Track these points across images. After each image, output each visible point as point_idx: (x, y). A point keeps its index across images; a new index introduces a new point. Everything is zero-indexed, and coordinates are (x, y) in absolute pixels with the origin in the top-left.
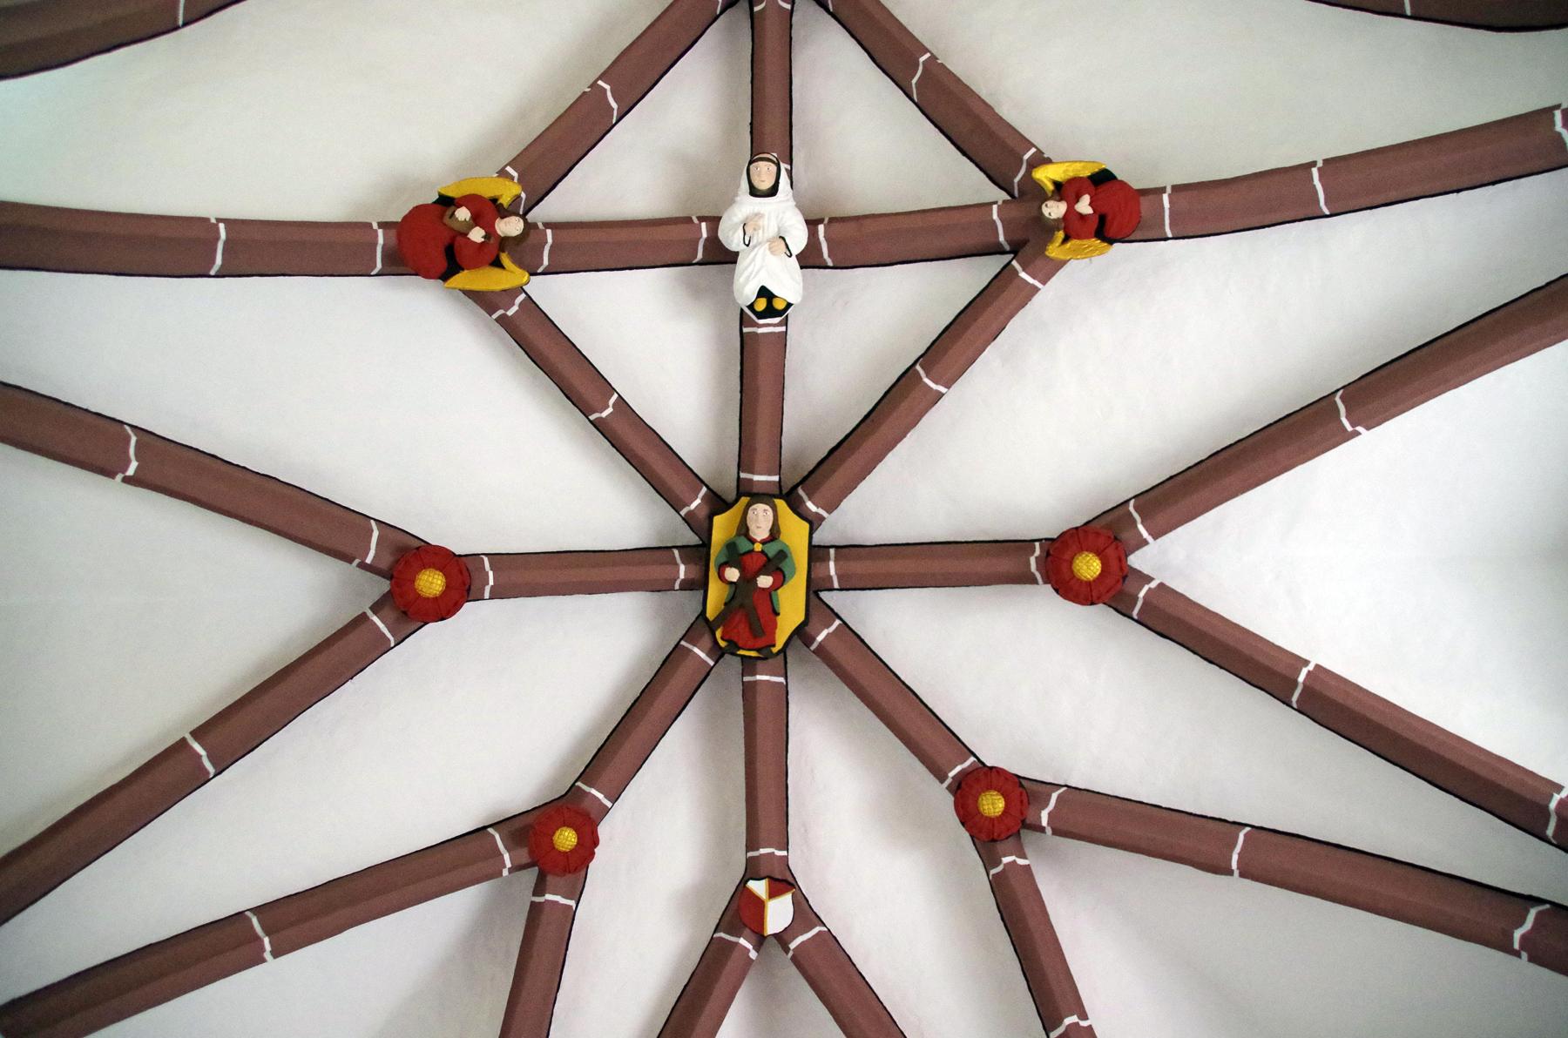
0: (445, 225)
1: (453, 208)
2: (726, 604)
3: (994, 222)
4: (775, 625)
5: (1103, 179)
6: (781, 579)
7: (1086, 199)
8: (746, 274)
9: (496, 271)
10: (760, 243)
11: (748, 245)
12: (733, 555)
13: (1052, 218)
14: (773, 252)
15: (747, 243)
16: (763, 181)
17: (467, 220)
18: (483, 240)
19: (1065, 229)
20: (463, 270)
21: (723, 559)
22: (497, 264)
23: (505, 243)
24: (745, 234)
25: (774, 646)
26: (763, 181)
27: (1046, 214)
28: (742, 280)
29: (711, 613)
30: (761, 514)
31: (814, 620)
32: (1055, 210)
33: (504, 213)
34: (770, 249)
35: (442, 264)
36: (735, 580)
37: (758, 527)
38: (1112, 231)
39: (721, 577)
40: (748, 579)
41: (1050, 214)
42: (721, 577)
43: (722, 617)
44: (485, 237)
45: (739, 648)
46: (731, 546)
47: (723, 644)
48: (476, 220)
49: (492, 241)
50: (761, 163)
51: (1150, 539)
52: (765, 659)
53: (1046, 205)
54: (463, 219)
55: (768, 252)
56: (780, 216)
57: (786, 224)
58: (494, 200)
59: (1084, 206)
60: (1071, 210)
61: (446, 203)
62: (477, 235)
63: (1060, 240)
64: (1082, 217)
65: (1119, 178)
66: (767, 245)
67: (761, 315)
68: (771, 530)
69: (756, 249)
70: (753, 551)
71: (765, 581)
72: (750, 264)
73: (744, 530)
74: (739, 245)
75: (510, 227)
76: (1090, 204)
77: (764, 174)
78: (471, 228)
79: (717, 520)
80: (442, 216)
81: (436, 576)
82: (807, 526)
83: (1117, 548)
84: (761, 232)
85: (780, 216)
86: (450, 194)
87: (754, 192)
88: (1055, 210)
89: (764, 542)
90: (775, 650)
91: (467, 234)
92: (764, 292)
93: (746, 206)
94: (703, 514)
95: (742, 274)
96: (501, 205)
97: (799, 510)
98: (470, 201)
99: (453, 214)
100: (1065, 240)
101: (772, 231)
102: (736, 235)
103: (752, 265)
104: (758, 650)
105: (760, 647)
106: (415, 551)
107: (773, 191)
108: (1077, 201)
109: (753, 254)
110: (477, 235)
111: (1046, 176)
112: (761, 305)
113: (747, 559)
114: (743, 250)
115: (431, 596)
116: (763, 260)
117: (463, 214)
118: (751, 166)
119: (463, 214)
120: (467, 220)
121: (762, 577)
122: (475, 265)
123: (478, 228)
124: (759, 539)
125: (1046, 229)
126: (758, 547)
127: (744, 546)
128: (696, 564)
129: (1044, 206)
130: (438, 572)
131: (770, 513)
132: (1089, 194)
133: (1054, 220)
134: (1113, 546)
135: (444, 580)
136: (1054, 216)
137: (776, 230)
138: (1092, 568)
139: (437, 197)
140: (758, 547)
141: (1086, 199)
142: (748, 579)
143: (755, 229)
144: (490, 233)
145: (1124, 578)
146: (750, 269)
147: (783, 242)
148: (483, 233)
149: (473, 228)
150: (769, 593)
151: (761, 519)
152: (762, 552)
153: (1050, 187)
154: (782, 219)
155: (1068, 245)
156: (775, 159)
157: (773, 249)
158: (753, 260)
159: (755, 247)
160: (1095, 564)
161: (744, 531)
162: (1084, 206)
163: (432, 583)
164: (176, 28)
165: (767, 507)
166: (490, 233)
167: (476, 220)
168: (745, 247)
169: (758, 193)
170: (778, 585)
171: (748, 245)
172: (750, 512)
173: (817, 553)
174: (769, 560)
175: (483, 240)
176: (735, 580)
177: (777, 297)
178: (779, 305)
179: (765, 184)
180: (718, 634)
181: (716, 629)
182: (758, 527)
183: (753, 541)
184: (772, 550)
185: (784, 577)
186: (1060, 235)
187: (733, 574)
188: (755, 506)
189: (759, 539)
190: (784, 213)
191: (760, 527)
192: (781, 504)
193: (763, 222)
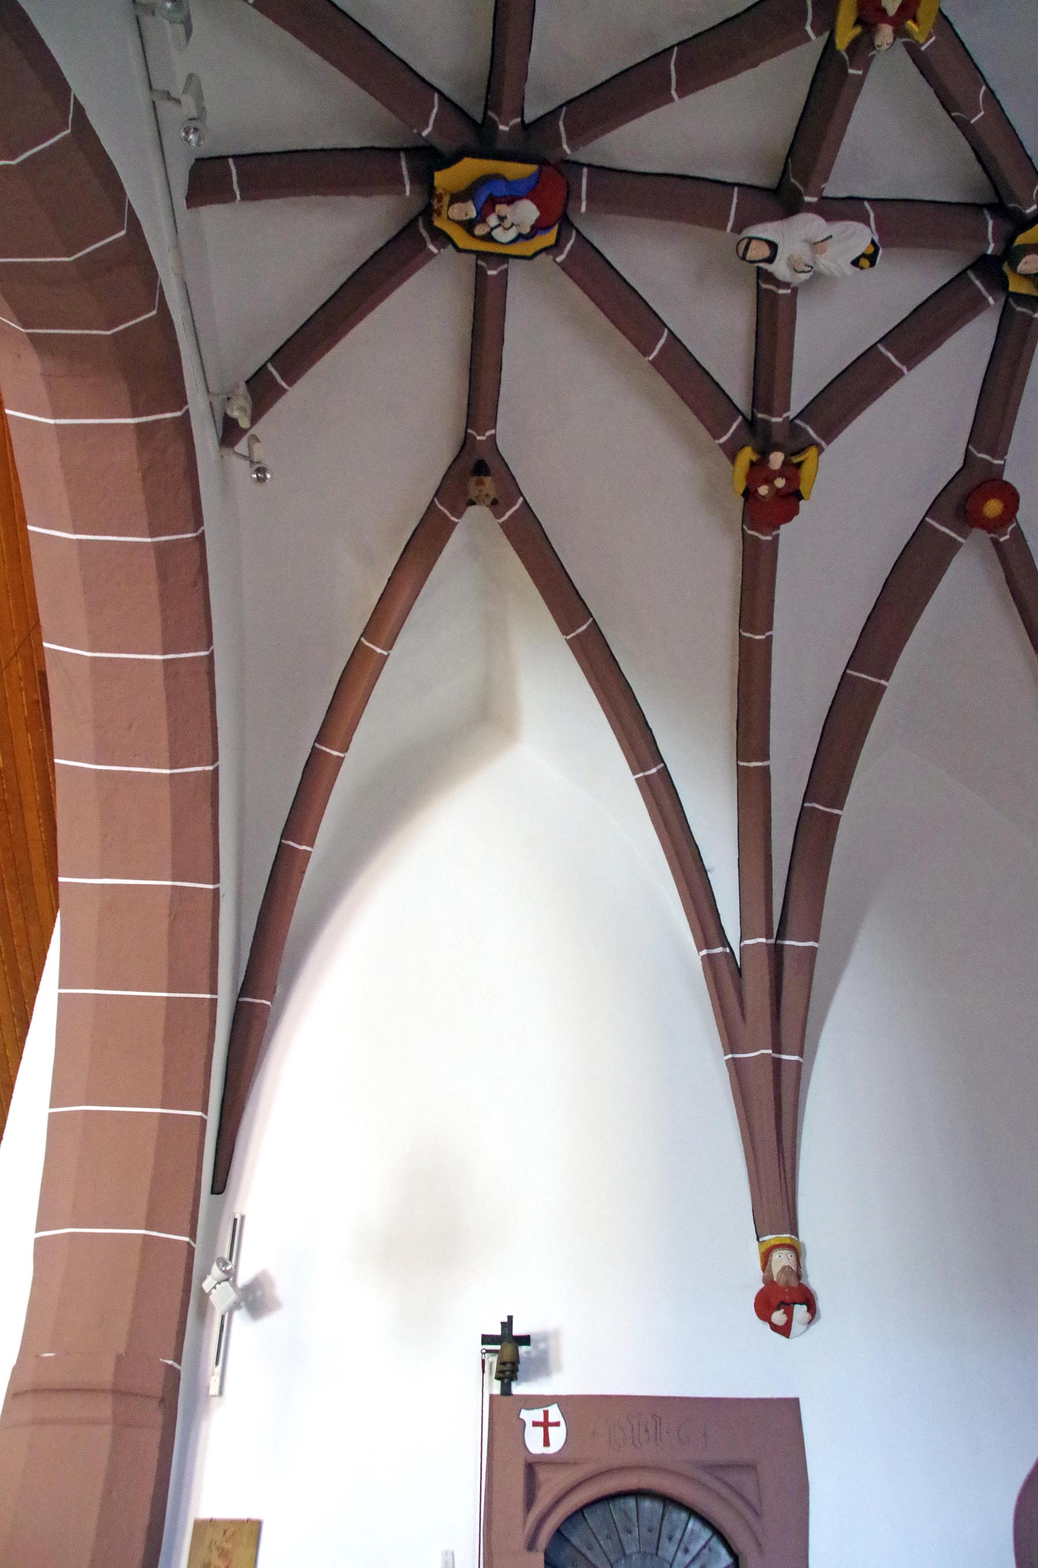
14: (823, 251)
15: (810, 269)
24: (803, 272)
44: (782, 478)
48: (769, 481)
55: (824, 255)
61: (749, 494)
78: (774, 486)
87: (771, 260)
99: (763, 497)
107: (773, 246)
117: (763, 490)
119: (763, 490)
156: (745, 242)
165: (1024, 260)
166: (780, 473)
167: (769, 481)
171: (812, 268)
179: (766, 252)
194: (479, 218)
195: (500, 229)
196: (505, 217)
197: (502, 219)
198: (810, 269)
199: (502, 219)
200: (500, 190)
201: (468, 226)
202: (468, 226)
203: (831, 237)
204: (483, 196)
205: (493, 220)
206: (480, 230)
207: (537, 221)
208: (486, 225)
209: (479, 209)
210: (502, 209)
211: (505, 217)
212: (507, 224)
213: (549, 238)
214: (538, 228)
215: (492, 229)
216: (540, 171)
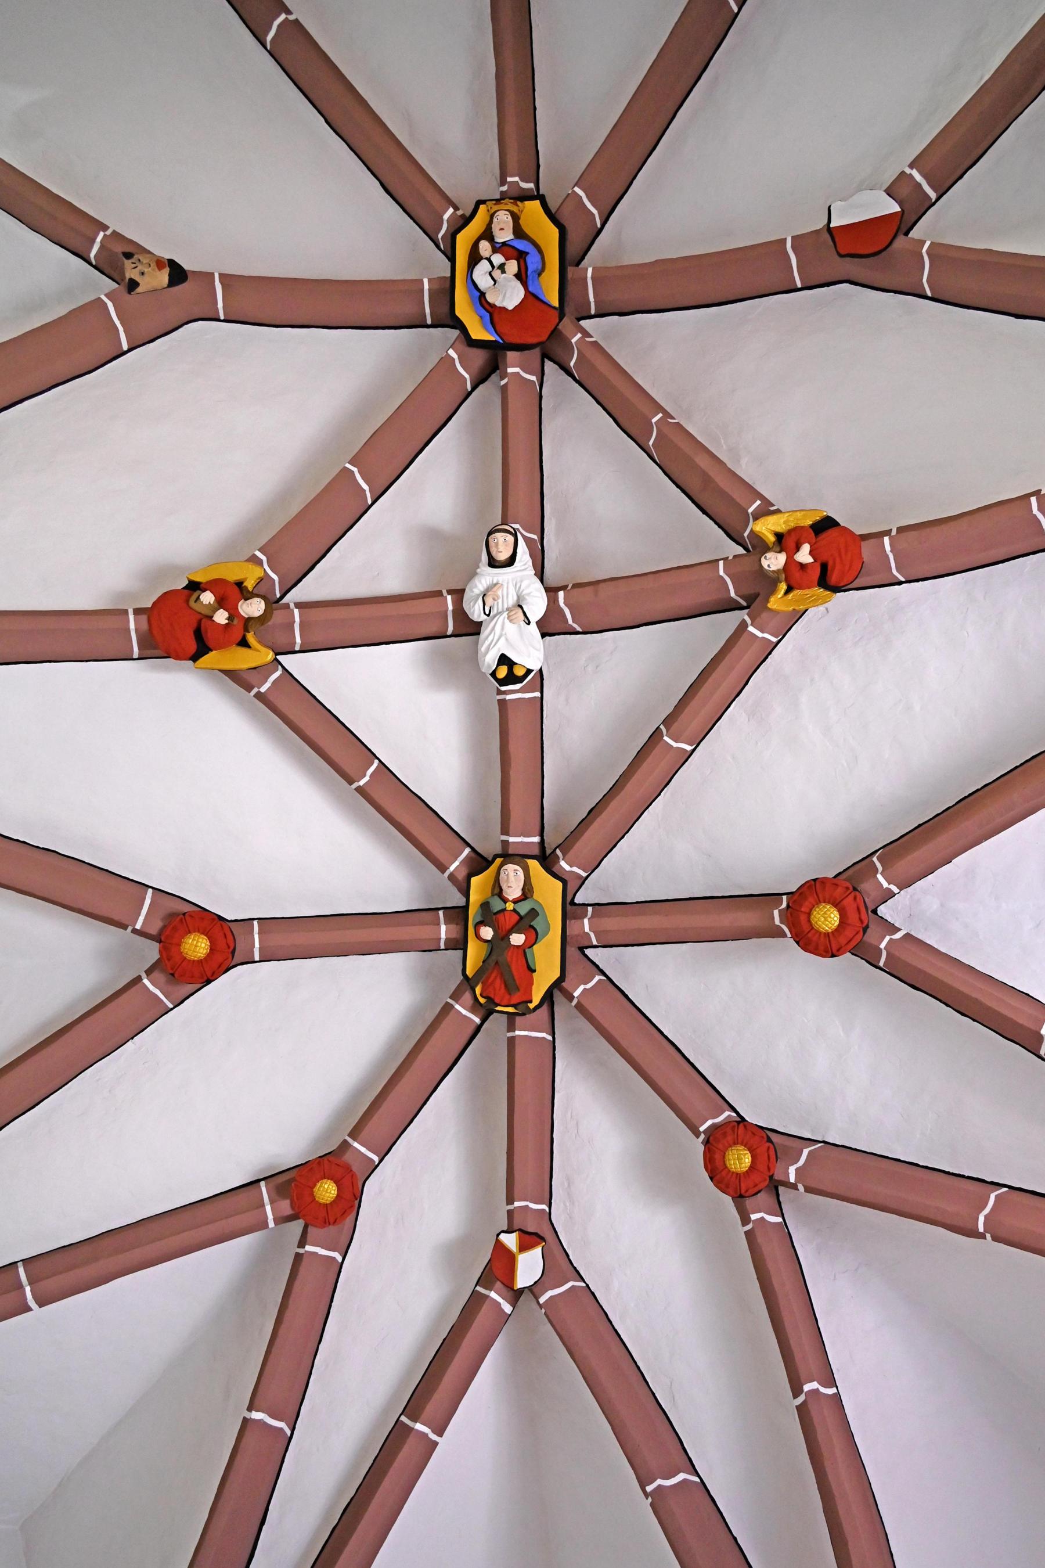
0: (191, 608)
1: (198, 592)
2: (483, 962)
4: (531, 983)
6: (534, 937)
7: (806, 548)
8: (487, 643)
10: (500, 612)
12: (488, 916)
13: (771, 569)
15: (487, 613)
16: (501, 552)
17: (212, 603)
18: (227, 621)
19: (786, 580)
20: (212, 651)
21: (479, 919)
22: (244, 643)
23: (248, 622)
24: (484, 604)
25: (531, 1002)
26: (501, 552)
27: (766, 567)
28: (483, 649)
29: (470, 972)
30: (512, 874)
31: (570, 976)
32: (775, 561)
33: (247, 595)
34: (508, 618)
35: (192, 647)
36: (489, 938)
37: (509, 887)
38: (833, 579)
39: (477, 935)
40: (502, 938)
41: (769, 566)
42: (477, 935)
43: (480, 973)
44: (228, 619)
45: (497, 1005)
46: (485, 906)
47: (482, 1000)
48: (221, 602)
49: (235, 622)
50: (498, 535)
52: (523, 1014)
53: (765, 558)
54: (207, 603)
55: (507, 621)
56: (518, 586)
57: (524, 593)
58: (239, 584)
59: (804, 556)
60: (790, 560)
61: (194, 587)
62: (221, 617)
63: (782, 592)
64: (803, 566)
66: (505, 614)
67: (503, 682)
68: (522, 890)
69: (497, 618)
70: (505, 910)
71: (517, 939)
72: (490, 634)
73: (498, 890)
74: (479, 616)
75: (253, 608)
76: (811, 553)
78: (215, 610)
79: (474, 880)
80: (187, 601)
81: (201, 940)
82: (560, 884)
83: (855, 898)
84: (500, 601)
85: (518, 586)
86: (197, 579)
87: (493, 563)
88: (775, 561)
89: (516, 901)
90: (532, 1006)
91: (212, 617)
92: (504, 660)
93: (487, 576)
94: (461, 876)
96: (246, 588)
97: (554, 870)
98: (214, 585)
99: (198, 598)
100: (787, 592)
101: (512, 600)
102: (476, 607)
103: (493, 634)
104: (514, 1006)
105: (515, 1003)
106: (182, 916)
107: (511, 561)
108: (798, 549)
110: (221, 617)
111: (767, 528)
112: (502, 673)
113: (501, 916)
114: (486, 620)
115: (196, 959)
116: (503, 628)
117: (208, 598)
118: (489, 538)
120: (212, 603)
121: (514, 934)
122: (221, 646)
123: (222, 610)
124: (511, 898)
125: (770, 581)
126: (510, 906)
127: (497, 905)
128: (457, 924)
129: (763, 558)
130: (203, 936)
131: (521, 873)
132: (809, 543)
134: (851, 897)
135: (208, 943)
136: (773, 568)
137: (515, 598)
138: (829, 919)
139: (187, 582)
140: (510, 906)
141: (806, 548)
142: (502, 938)
143: (494, 599)
144: (233, 615)
145: (865, 929)
146: (490, 638)
147: (520, 611)
148: (226, 614)
149: (218, 610)
150: (523, 950)
151: (513, 879)
152: (514, 910)
153: (772, 539)
154: (520, 587)
155: (790, 596)
157: (511, 618)
158: (493, 629)
159: (495, 616)
160: (832, 916)
161: (497, 891)
162: (804, 556)
163: (196, 946)
165: (517, 867)
166: (233, 615)
167: (221, 602)
168: (486, 617)
169: (497, 564)
170: (530, 943)
171: (488, 615)
172: (502, 871)
173: (570, 909)
174: (521, 918)
175: (227, 621)
176: (490, 939)
177: (516, 664)
178: (519, 672)
179: (503, 555)
180: (478, 990)
181: (476, 985)
182: (509, 887)
183: (505, 901)
184: (524, 908)
185: (537, 937)
186: (783, 587)
187: (487, 933)
188: (505, 867)
189: (511, 898)
190: (521, 581)
191: (513, 889)
192: (534, 865)
194: (498, 246)
195: (490, 268)
196: (503, 272)
197: (502, 267)
198: (487, 613)
199: (502, 267)
200: (533, 262)
201: (487, 234)
202: (487, 234)
203: (529, 623)
204: (521, 245)
205: (498, 259)
206: (485, 247)
207: (504, 309)
208: (491, 253)
209: (507, 243)
210: (513, 266)
211: (503, 272)
212: (497, 273)
213: (479, 332)
214: (492, 313)
215: (489, 260)
216: (554, 308)
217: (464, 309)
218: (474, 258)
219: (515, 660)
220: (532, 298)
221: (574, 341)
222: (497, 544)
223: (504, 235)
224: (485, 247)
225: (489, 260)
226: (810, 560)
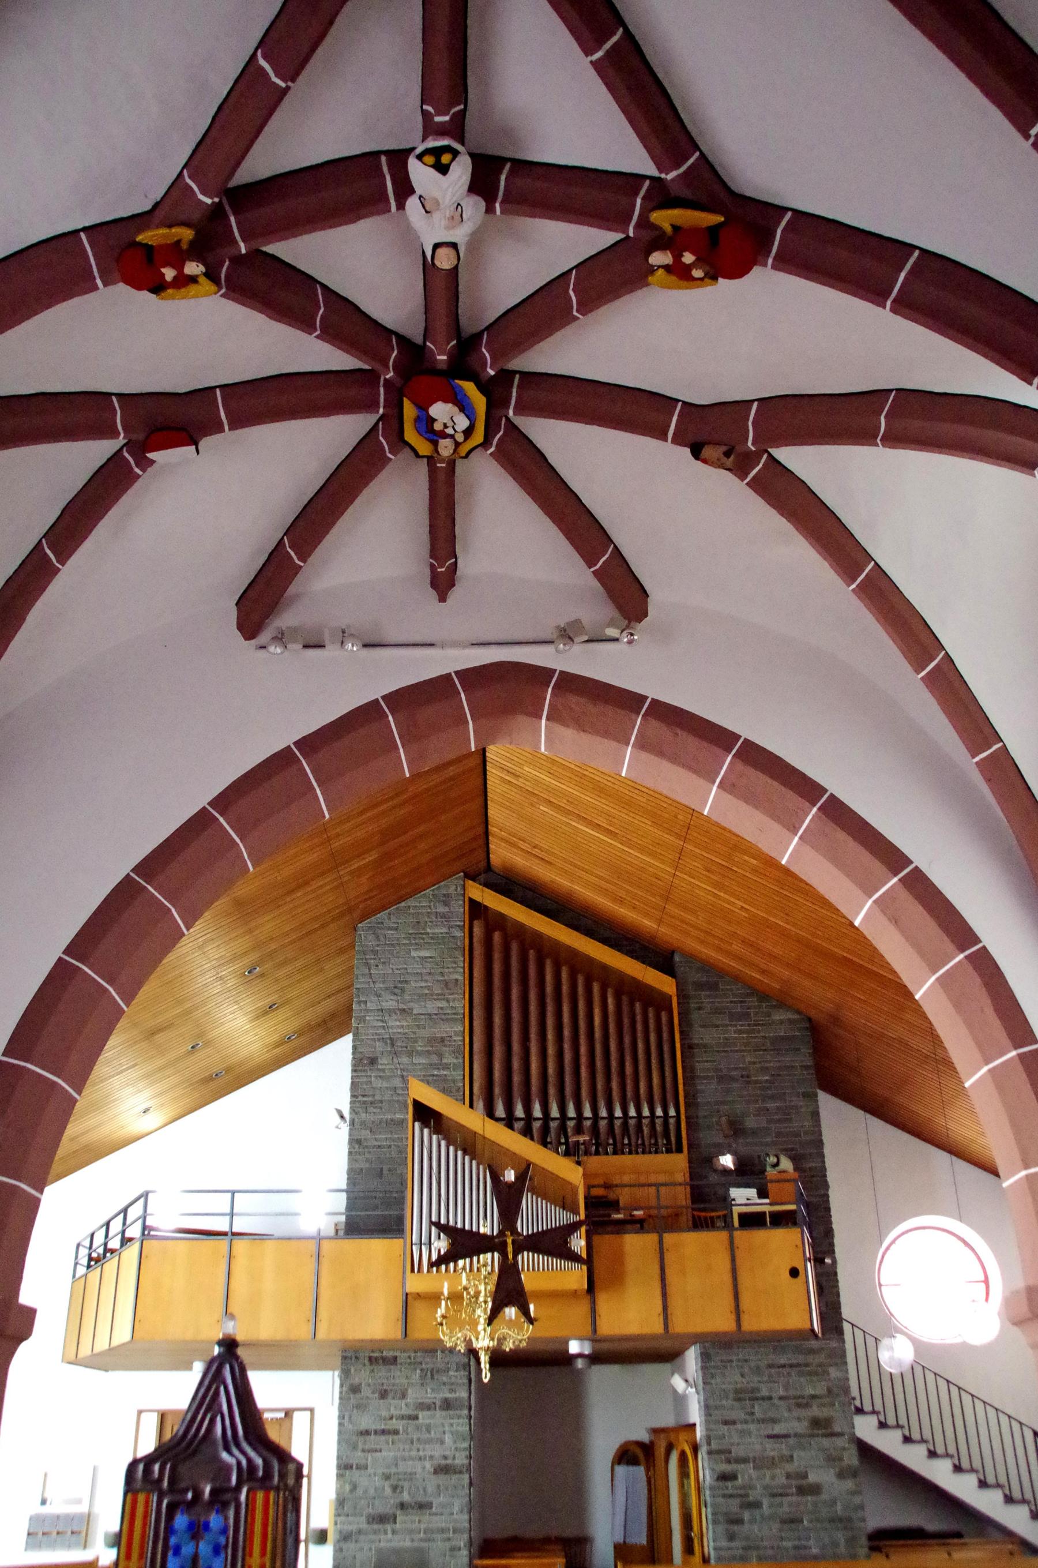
3: (244, 241)
5: (158, 288)
8: (460, 184)
9: (679, 223)
11: (459, 204)
14: (437, 203)
15: (459, 207)
22: (675, 228)
27: (200, 265)
51: (207, 807)
62: (688, 258)
65: (145, 292)
76: (164, 275)
77: (445, 260)
84: (448, 215)
87: (454, 246)
92: (443, 169)
93: (460, 235)
95: (462, 185)
101: (436, 216)
107: (436, 246)
109: (455, 199)
112: (445, 159)
133: (193, 261)
144: (678, 257)
147: (427, 209)
164: (897, 390)
166: (678, 257)
167: (689, 268)
168: (461, 203)
171: (459, 204)
177: (431, 166)
178: (430, 159)
193: (443, 223)
199: (445, 426)
201: (457, 445)
205: (450, 431)
210: (438, 427)
217: (479, 402)
218: (468, 432)
219: (432, 170)
220: (423, 407)
221: (392, 374)
222: (449, 259)
223: (443, 443)
224: (460, 438)
225: (455, 431)
226: (163, 270)
